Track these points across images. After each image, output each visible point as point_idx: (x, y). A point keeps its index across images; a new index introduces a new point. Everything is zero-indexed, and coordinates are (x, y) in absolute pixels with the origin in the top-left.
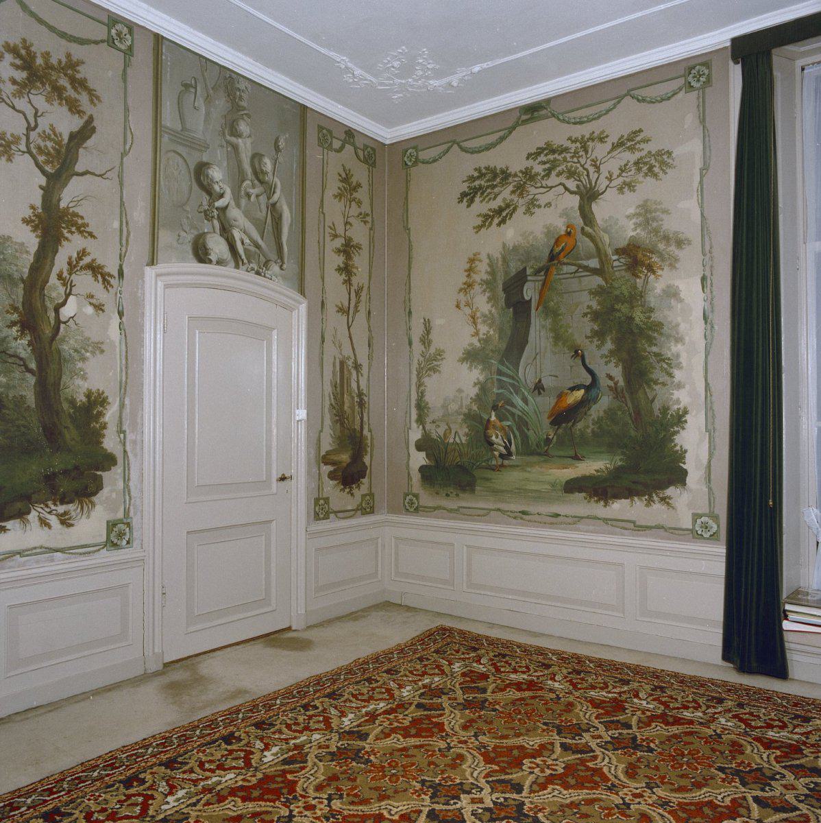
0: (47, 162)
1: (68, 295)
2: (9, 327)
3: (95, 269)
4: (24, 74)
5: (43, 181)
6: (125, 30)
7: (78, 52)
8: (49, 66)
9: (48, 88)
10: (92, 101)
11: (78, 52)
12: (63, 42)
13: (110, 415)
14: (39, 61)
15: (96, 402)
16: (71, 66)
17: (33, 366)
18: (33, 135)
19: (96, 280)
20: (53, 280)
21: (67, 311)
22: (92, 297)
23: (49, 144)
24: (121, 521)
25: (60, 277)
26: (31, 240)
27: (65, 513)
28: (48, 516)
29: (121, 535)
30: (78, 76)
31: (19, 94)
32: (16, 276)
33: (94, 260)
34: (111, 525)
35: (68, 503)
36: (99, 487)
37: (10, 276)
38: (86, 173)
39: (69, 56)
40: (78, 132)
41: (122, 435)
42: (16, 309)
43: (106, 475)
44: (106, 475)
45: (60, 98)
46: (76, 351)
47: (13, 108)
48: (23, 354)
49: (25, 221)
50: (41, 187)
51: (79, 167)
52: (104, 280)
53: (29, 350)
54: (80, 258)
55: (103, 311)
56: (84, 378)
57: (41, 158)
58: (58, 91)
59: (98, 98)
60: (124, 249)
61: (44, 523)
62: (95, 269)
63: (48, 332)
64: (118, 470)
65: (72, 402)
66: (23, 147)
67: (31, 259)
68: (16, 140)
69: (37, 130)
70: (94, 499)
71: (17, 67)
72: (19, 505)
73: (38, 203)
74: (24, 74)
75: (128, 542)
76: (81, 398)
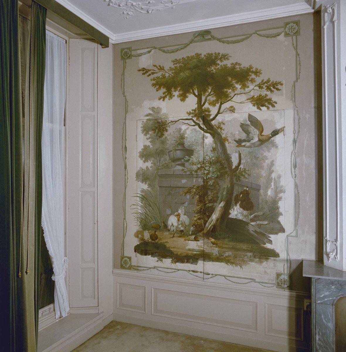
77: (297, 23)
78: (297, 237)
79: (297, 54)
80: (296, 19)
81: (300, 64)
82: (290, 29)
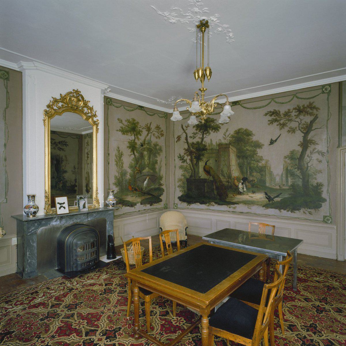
0: (304, 130)
1: (310, 160)
2: (295, 169)
3: (319, 152)
4: (298, 113)
5: (303, 135)
6: (328, 86)
7: (312, 100)
8: (304, 108)
9: (304, 113)
10: (317, 111)
11: (312, 100)
12: (308, 100)
13: (324, 189)
14: (302, 108)
15: (319, 186)
16: (311, 104)
17: (301, 177)
18: (300, 125)
19: (319, 154)
20: (306, 157)
21: (309, 165)
22: (318, 159)
23: (304, 126)
24: (328, 216)
25: (308, 156)
26: (300, 149)
27: (310, 211)
28: (306, 211)
29: (328, 220)
30: (313, 106)
31: (297, 117)
32: (296, 158)
33: (318, 150)
34: (325, 217)
35: (312, 209)
36: (321, 207)
37: (295, 158)
38: (316, 129)
39: (310, 103)
40: (313, 120)
41: (328, 194)
42: (296, 165)
43: (323, 204)
44: (323, 204)
45: (307, 114)
46: (313, 173)
47: (295, 121)
48: (299, 175)
49: (299, 145)
50: (302, 136)
51: (313, 129)
52: (322, 154)
53: (300, 174)
54: (314, 150)
55: (322, 162)
56: (316, 179)
57: (302, 130)
58: (307, 113)
59: (319, 109)
60: (329, 145)
61: (304, 212)
62: (319, 152)
63: (305, 169)
64: (327, 203)
65: (312, 185)
66: (298, 129)
67: (300, 153)
68: (296, 128)
69: (302, 123)
70: (319, 209)
71: (295, 112)
72: (298, 208)
73: (302, 140)
74: (298, 113)
75: (331, 222)
76: (315, 184)
77: (8, 73)
78: (7, 202)
79: (7, 92)
80: (7, 70)
81: (9, 98)
82: (2, 74)
